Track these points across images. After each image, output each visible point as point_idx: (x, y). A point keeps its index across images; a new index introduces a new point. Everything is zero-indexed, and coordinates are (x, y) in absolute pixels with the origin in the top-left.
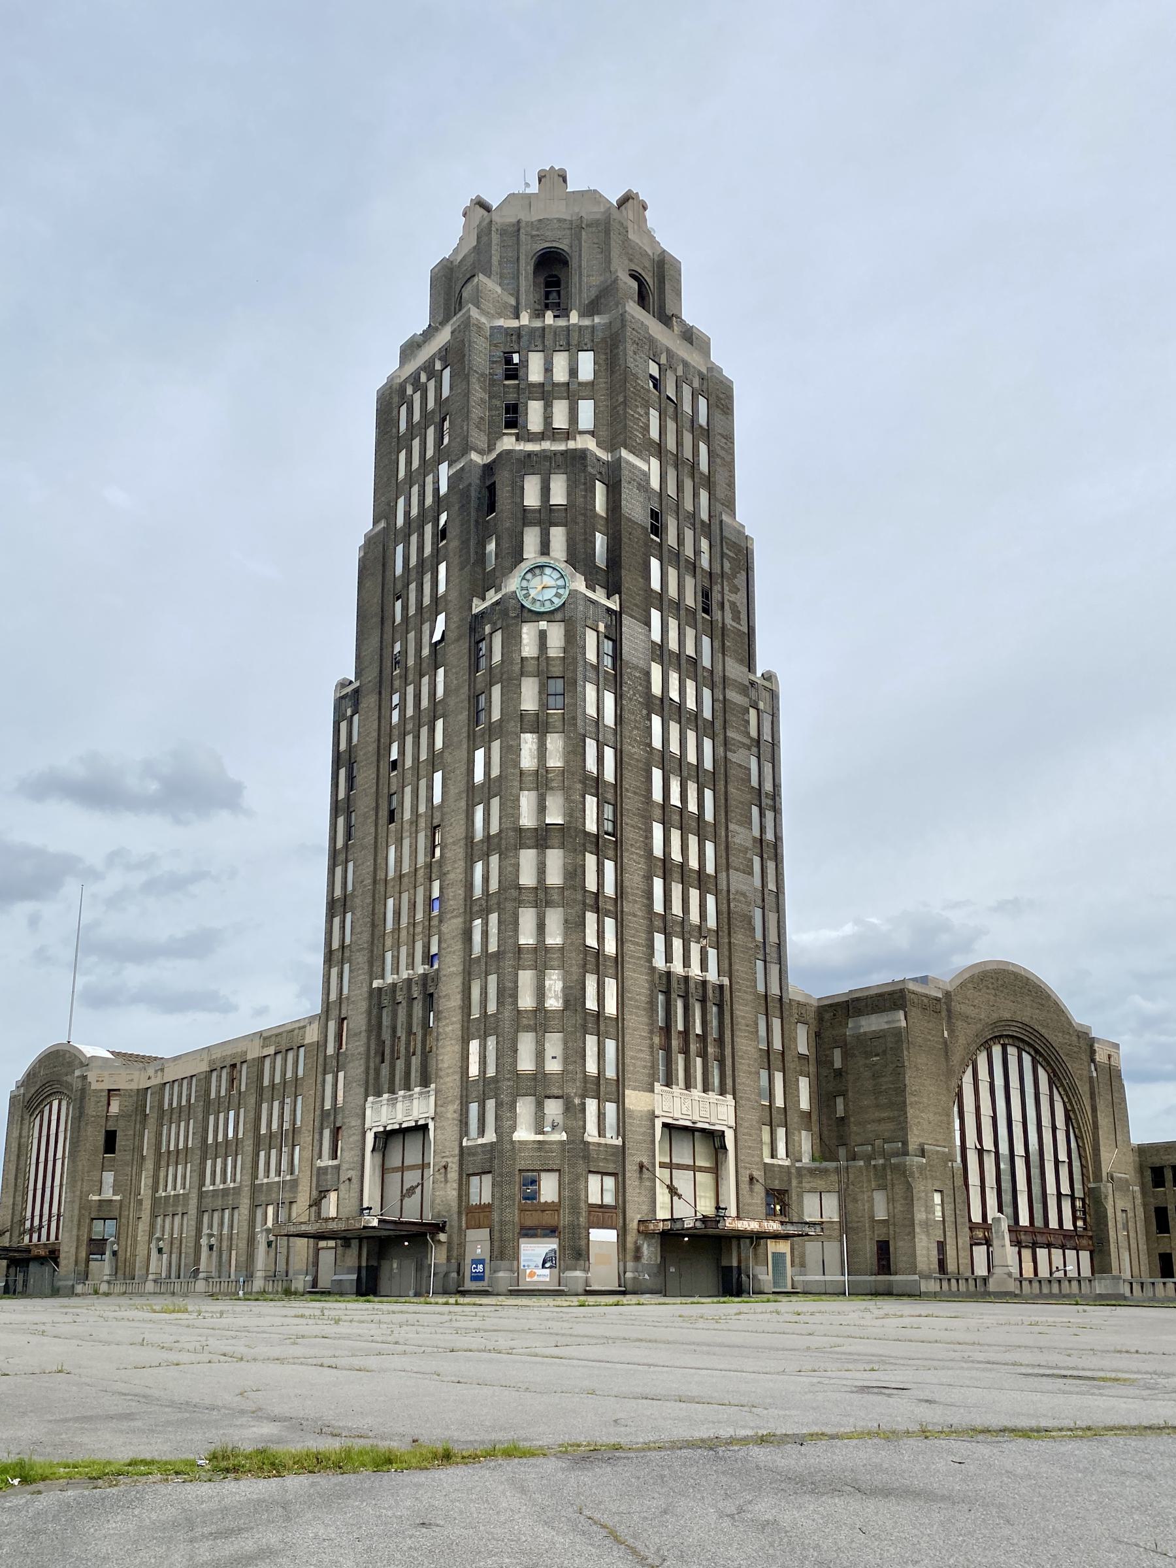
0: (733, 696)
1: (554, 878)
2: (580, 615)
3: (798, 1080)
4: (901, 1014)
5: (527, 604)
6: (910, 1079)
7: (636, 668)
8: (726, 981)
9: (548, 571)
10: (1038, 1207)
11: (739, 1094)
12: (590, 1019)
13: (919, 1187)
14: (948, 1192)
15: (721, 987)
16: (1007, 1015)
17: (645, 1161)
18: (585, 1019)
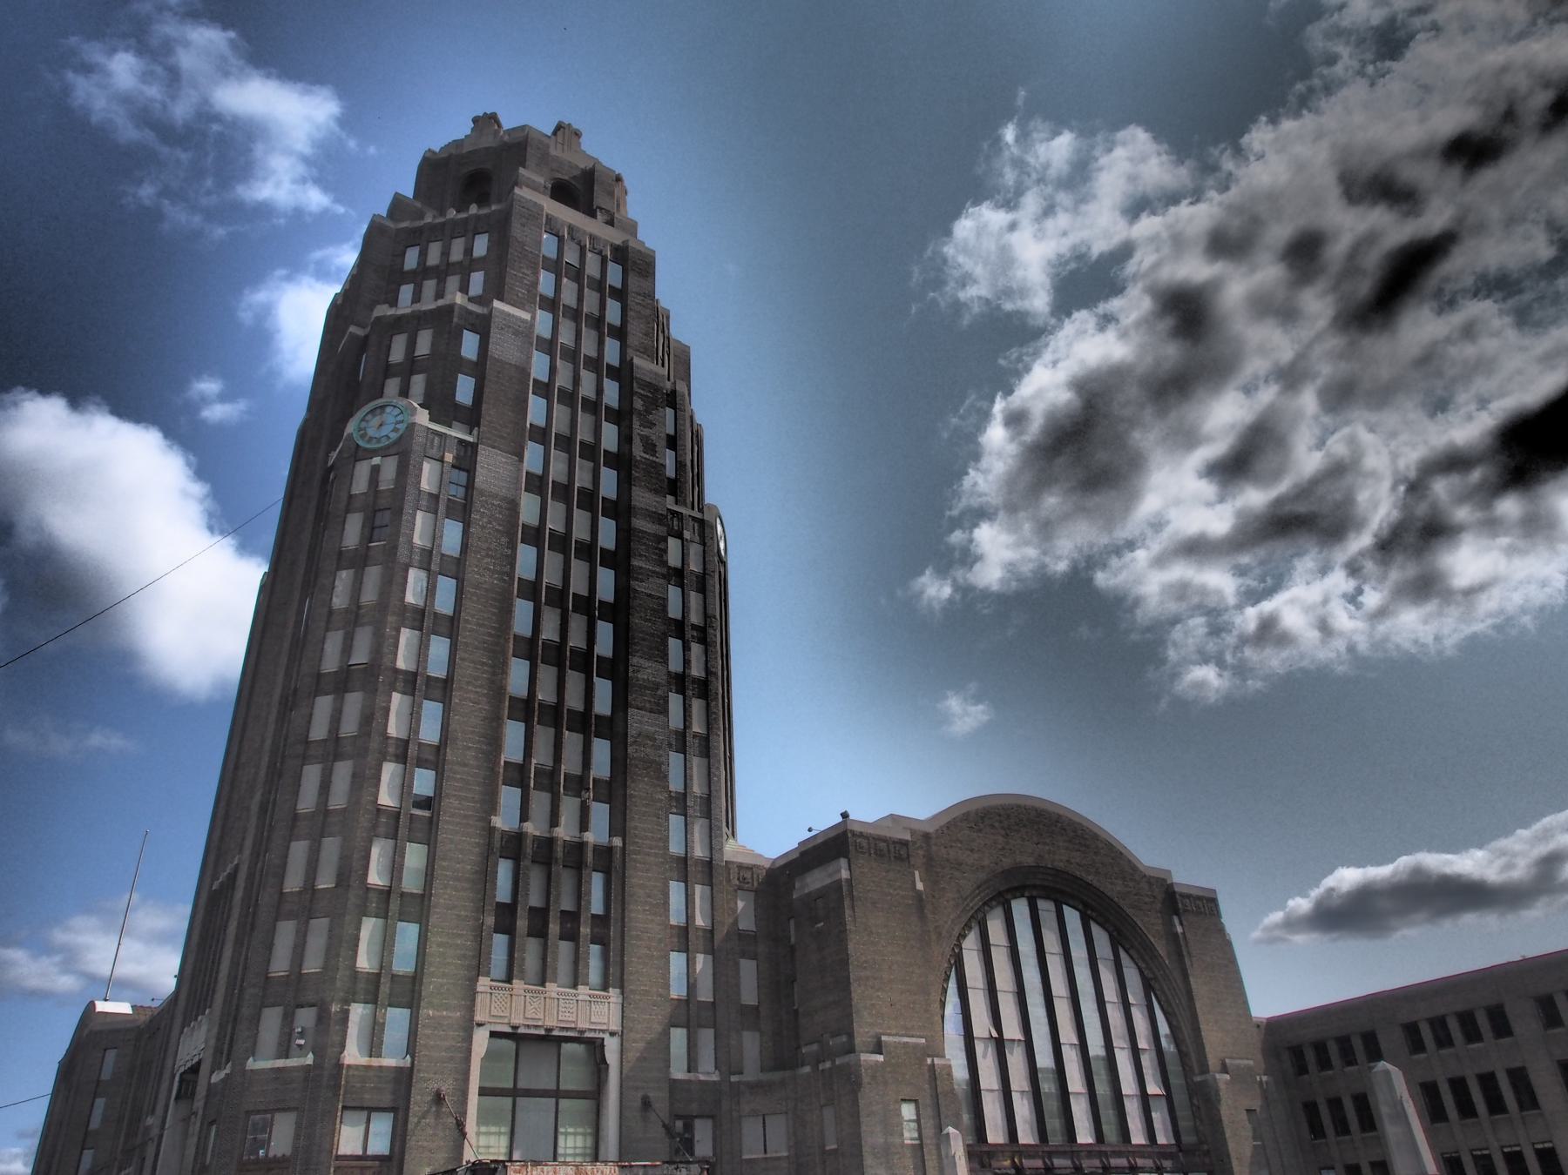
0: (639, 523)
1: (349, 727)
2: (416, 448)
3: (737, 964)
4: (843, 862)
5: (361, 443)
6: (857, 947)
7: (495, 496)
8: (617, 842)
9: (388, 410)
10: (1108, 1115)
11: (629, 987)
12: (373, 896)
13: (869, 1097)
14: (926, 1100)
15: (610, 850)
16: (1029, 861)
17: (447, 1087)
18: (366, 899)
